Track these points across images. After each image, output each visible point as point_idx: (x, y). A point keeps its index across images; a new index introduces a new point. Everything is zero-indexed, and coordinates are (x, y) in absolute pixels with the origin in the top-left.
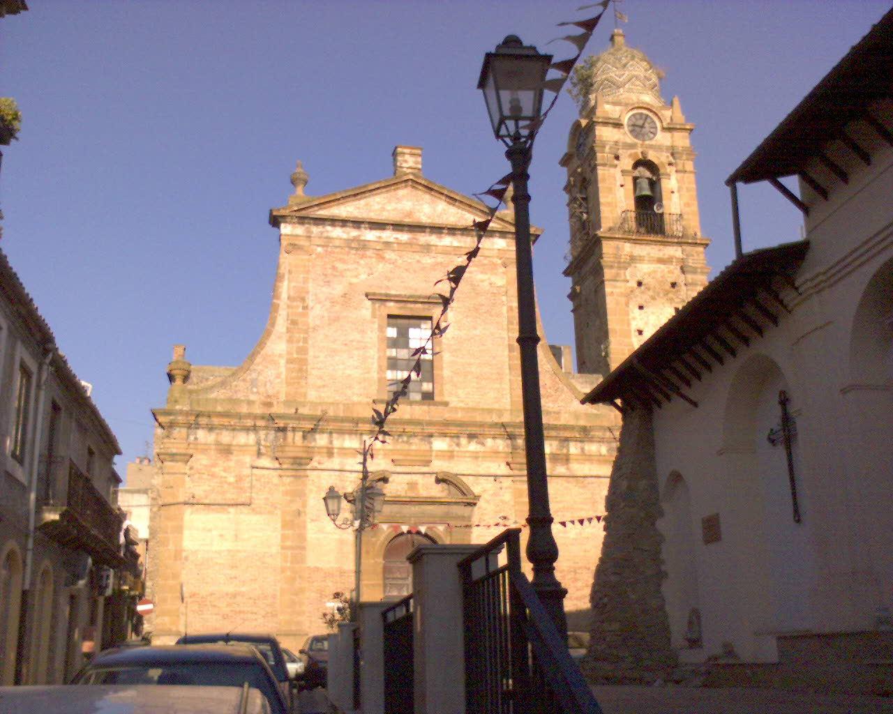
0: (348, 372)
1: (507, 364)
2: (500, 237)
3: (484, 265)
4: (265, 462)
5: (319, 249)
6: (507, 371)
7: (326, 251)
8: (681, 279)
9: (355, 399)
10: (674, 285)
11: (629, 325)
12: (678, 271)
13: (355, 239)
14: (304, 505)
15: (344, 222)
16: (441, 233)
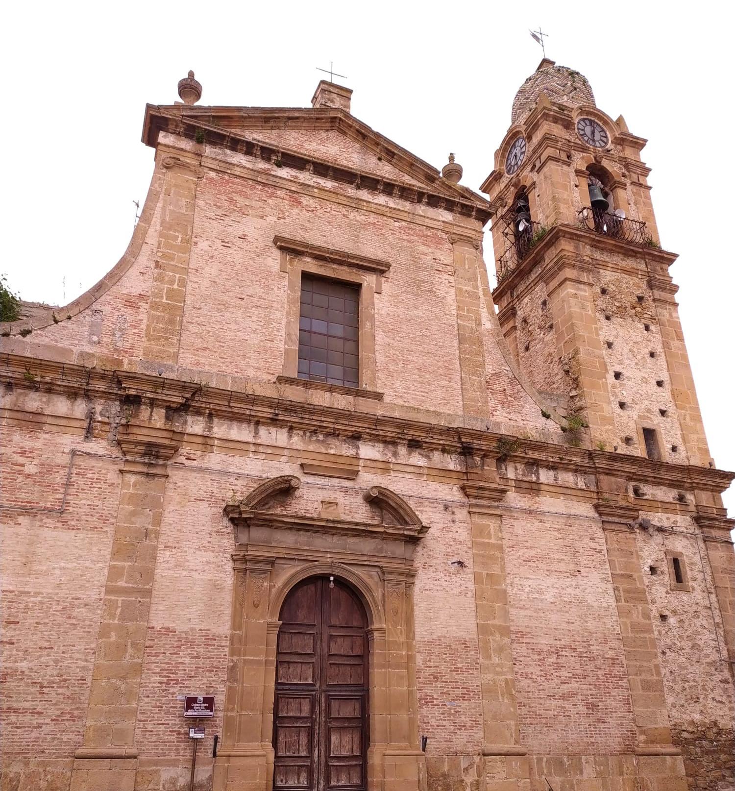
0: (242, 335)
1: (457, 357)
2: (446, 209)
3: (426, 236)
4: (98, 446)
5: (212, 174)
6: (457, 367)
7: (222, 178)
9: (251, 373)
10: (640, 299)
11: (598, 335)
12: (644, 284)
13: (265, 173)
14: (158, 520)
15: (249, 148)
16: (375, 189)
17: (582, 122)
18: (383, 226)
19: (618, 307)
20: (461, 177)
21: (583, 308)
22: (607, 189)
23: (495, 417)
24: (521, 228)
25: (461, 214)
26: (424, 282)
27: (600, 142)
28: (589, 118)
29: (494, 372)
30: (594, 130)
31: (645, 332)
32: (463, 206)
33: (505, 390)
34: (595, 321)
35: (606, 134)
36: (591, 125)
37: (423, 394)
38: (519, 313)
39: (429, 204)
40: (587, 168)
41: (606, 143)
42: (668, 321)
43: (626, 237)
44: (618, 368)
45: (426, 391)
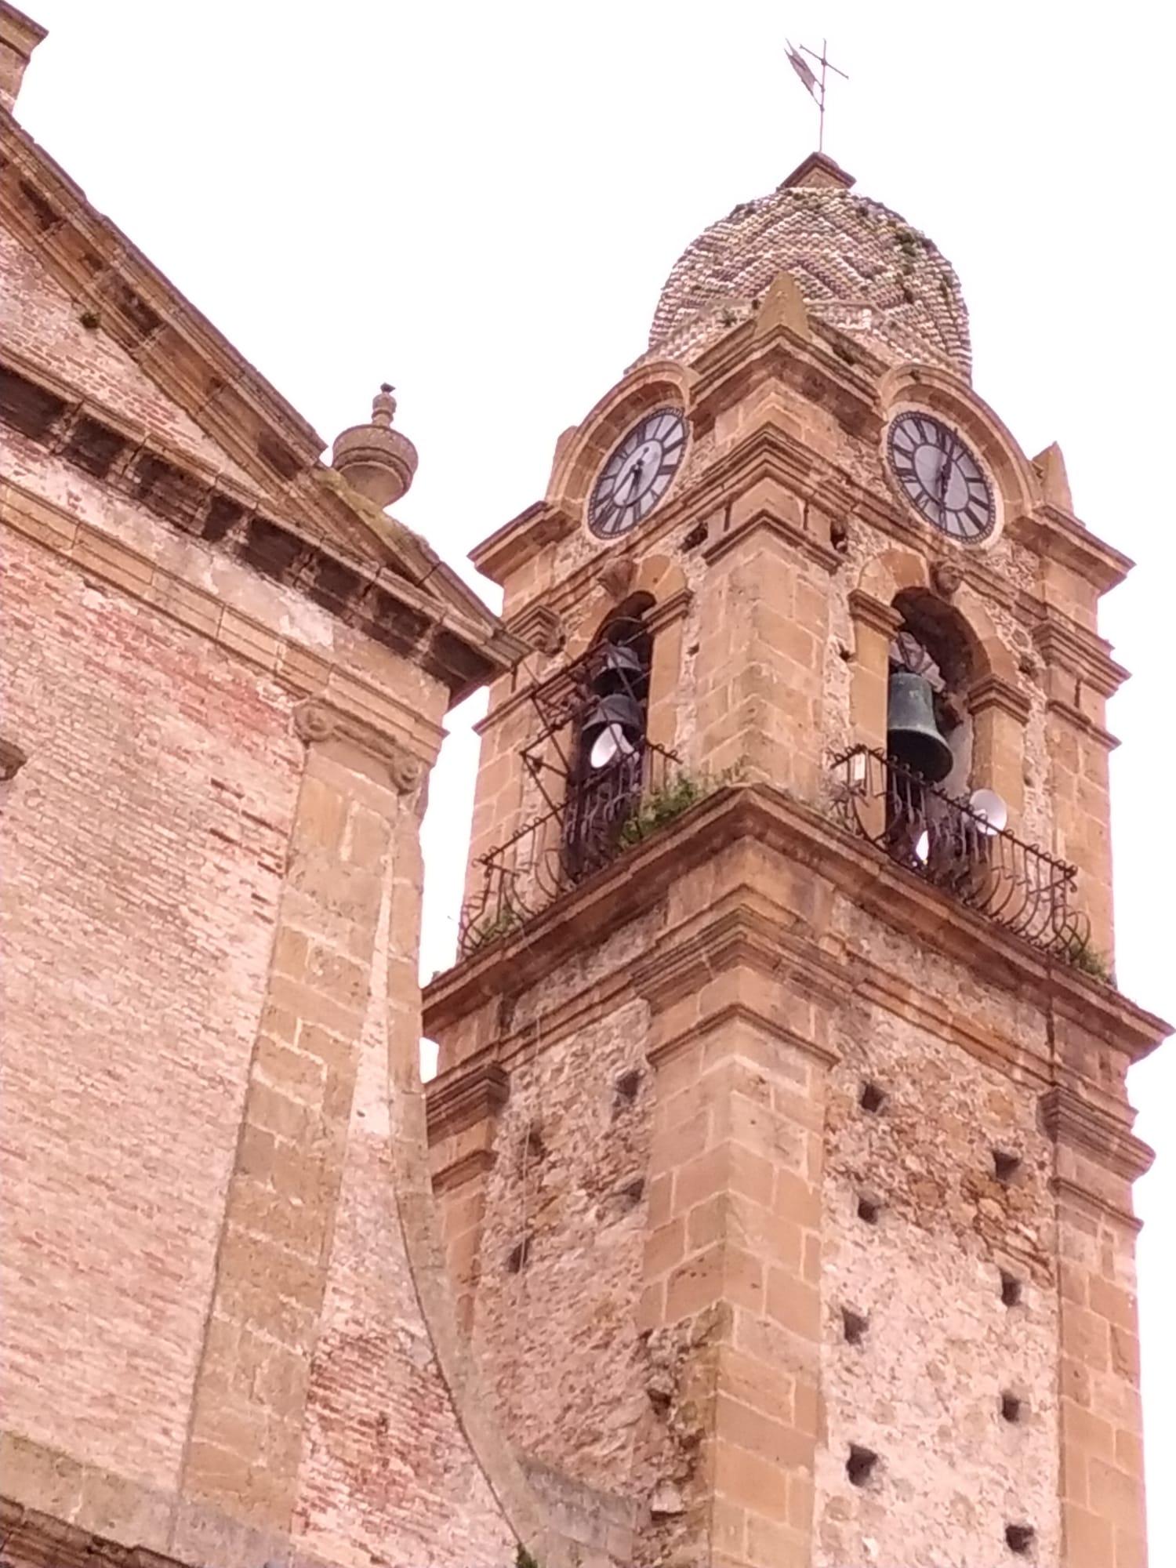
1: (210, 1229)
2: (314, 595)
3: (204, 681)
6: (203, 1271)
8: (1034, 1149)
10: (1005, 1165)
11: (815, 1271)
12: (1028, 1110)
16: (39, 432)
17: (909, 425)
18: (32, 590)
19: (914, 1178)
20: (406, 488)
21: (780, 1145)
22: (954, 700)
23: (312, 1536)
24: (600, 756)
25: (374, 632)
26: (148, 867)
27: (963, 516)
28: (941, 417)
29: (353, 1330)
30: (947, 467)
31: (1000, 1306)
32: (387, 603)
33: (383, 1421)
34: (814, 1210)
35: (989, 495)
36: (941, 446)
37: (19, 1358)
38: (518, 1100)
39: (248, 556)
40: (899, 600)
41: (984, 529)
42: (1094, 1281)
43: (995, 906)
44: (869, 1435)
45: (36, 1345)
